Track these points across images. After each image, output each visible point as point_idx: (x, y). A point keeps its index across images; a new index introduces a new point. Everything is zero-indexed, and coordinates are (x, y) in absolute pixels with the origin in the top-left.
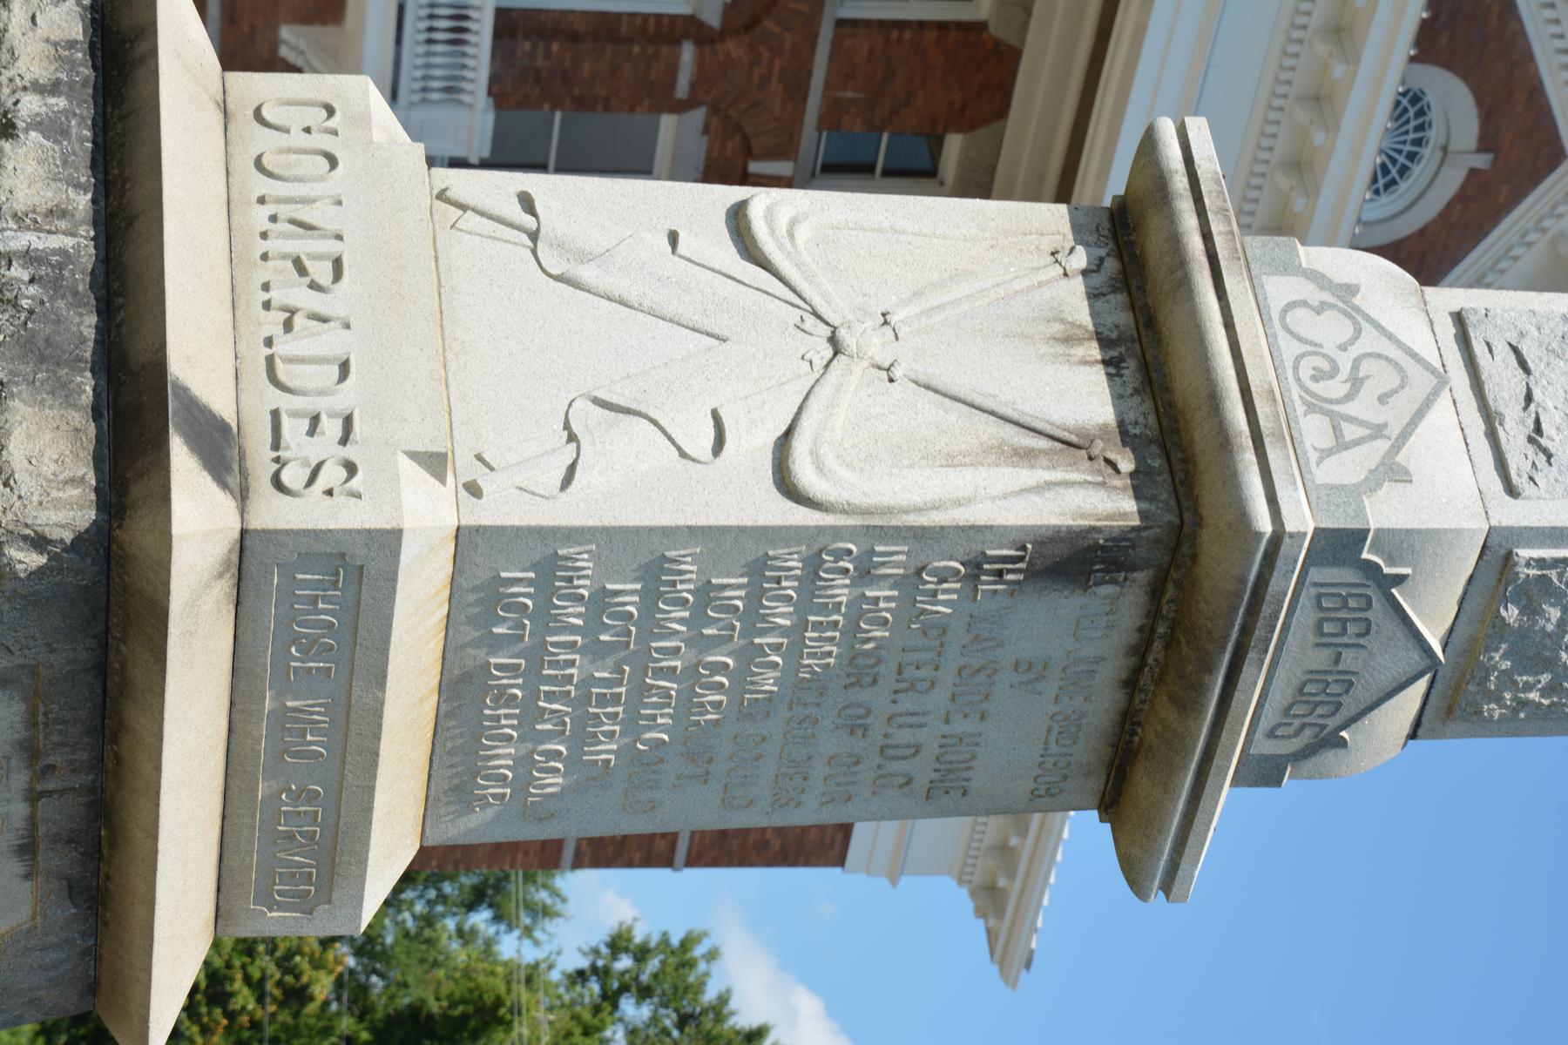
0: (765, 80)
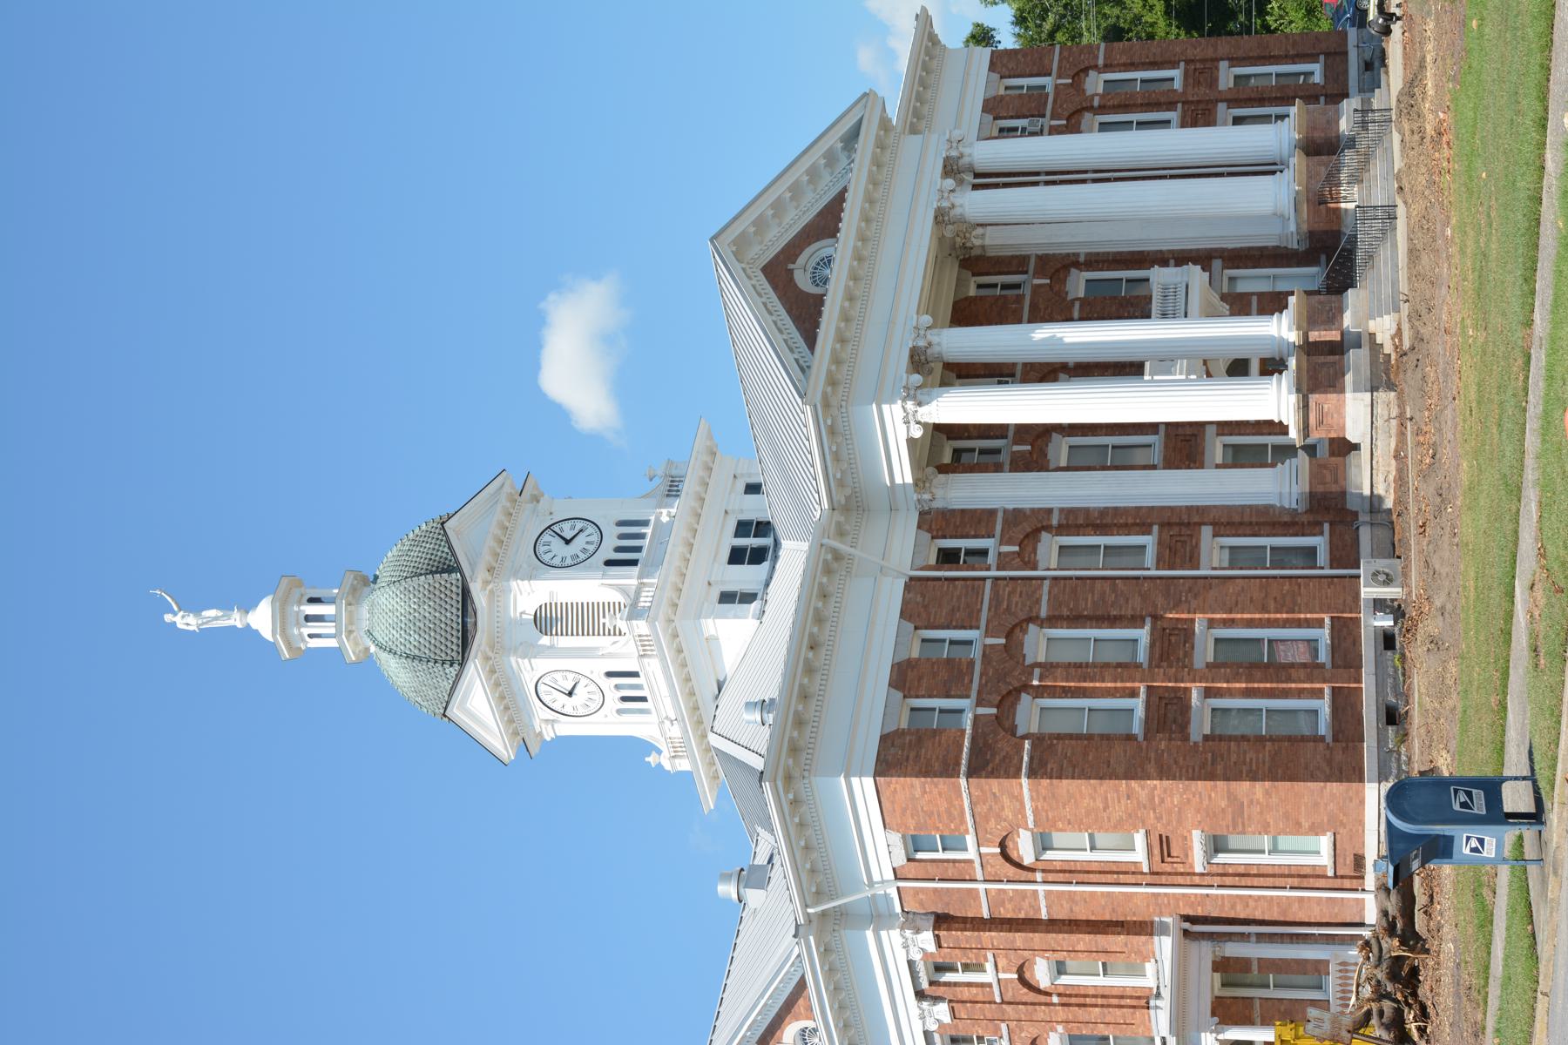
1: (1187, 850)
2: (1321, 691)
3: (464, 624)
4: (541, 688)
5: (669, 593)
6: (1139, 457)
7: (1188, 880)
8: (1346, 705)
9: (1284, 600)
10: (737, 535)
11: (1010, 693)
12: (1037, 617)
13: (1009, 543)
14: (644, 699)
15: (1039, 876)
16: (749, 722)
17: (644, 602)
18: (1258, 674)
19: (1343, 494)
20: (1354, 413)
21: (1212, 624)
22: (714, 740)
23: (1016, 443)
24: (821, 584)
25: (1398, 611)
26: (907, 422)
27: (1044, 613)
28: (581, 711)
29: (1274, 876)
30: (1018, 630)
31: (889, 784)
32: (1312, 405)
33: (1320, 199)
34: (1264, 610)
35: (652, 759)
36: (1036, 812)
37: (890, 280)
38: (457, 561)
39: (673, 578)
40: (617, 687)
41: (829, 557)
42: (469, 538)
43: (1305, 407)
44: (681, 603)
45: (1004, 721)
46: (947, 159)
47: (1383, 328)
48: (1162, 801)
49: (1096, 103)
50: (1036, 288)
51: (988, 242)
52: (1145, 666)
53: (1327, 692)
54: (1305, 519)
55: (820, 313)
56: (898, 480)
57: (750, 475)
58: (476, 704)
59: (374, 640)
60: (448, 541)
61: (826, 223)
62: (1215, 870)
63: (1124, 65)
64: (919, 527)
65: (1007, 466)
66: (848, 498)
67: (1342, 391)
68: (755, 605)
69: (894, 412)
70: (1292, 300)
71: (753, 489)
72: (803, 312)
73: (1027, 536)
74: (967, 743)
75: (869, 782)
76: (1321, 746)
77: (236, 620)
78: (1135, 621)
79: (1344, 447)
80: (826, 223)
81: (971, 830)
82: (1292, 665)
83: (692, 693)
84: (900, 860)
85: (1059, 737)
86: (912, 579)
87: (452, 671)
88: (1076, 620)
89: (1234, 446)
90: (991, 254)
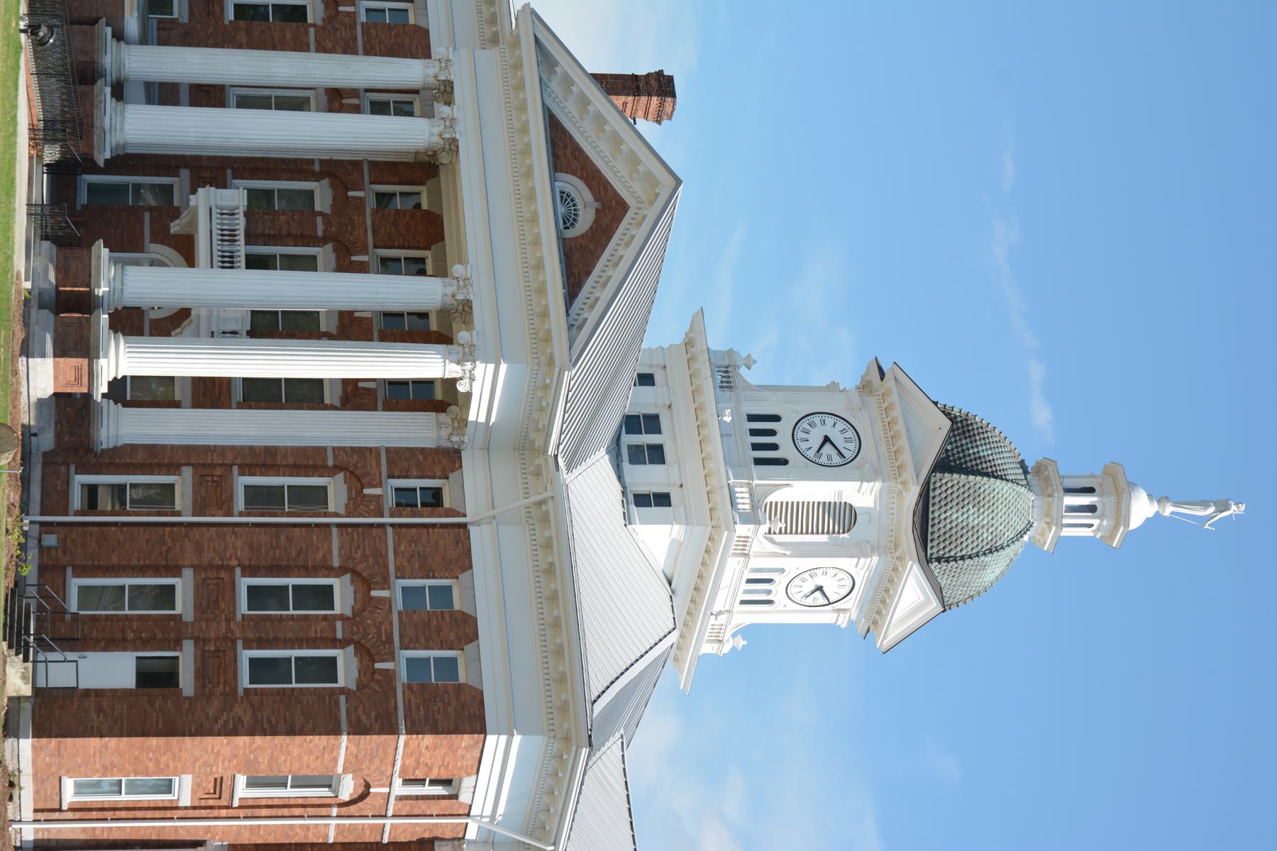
40: (774, 447)
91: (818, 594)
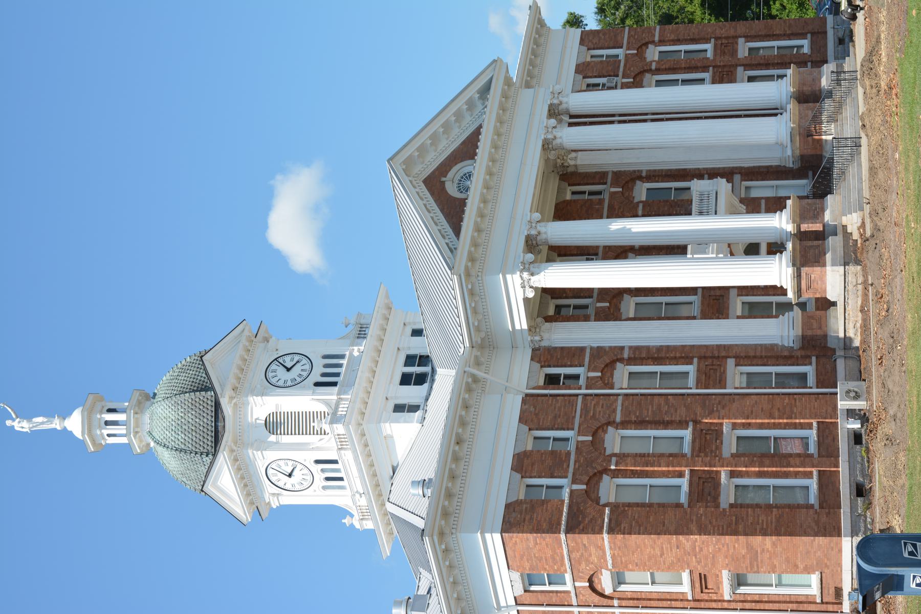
0: (619, 208)
1: (719, 584)
2: (811, 473)
3: (216, 427)
4: (270, 471)
5: (358, 405)
6: (684, 310)
7: (719, 605)
8: (828, 483)
9: (784, 410)
10: (405, 365)
11: (595, 474)
12: (614, 422)
13: (594, 371)
14: (341, 479)
15: (616, 603)
16: (414, 495)
17: (341, 411)
18: (767, 461)
19: (825, 336)
20: (833, 280)
21: (735, 426)
22: (390, 508)
23: (598, 301)
24: (464, 399)
25: (863, 418)
26: (523, 287)
27: (618, 419)
28: (298, 487)
29: (779, 602)
30: (600, 431)
31: (511, 538)
32: (803, 275)
33: (807, 133)
34: (771, 416)
35: (347, 521)
36: (613, 557)
37: (512, 189)
38: (211, 383)
39: (362, 395)
40: (323, 470)
41: (470, 380)
42: (220, 368)
43: (798, 276)
44: (367, 412)
45: (591, 494)
46: (551, 105)
47: (852, 222)
48: (701, 550)
49: (653, 67)
50: (612, 195)
51: (579, 162)
52: (689, 455)
53: (815, 474)
54: (799, 354)
55: (463, 212)
56: (518, 327)
57: (415, 323)
58: (224, 483)
59: (153, 438)
60: (205, 369)
61: (467, 150)
62: (738, 598)
63: (673, 41)
64: (532, 359)
65: (593, 317)
66: (482, 339)
67: (824, 265)
68: (418, 414)
69: (514, 281)
70: (789, 203)
71: (417, 333)
72: (452, 211)
73: (607, 366)
74: (565, 509)
75: (497, 537)
76: (811, 512)
77: (56, 424)
78: (681, 424)
79: (826, 304)
80: (467, 150)
81: (569, 570)
82: (790, 455)
83: (375, 475)
84: (519, 591)
85: (629, 505)
86: (527, 395)
87: (208, 460)
88: (641, 424)
89: (749, 303)
90: (581, 170)
91: (289, 367)
